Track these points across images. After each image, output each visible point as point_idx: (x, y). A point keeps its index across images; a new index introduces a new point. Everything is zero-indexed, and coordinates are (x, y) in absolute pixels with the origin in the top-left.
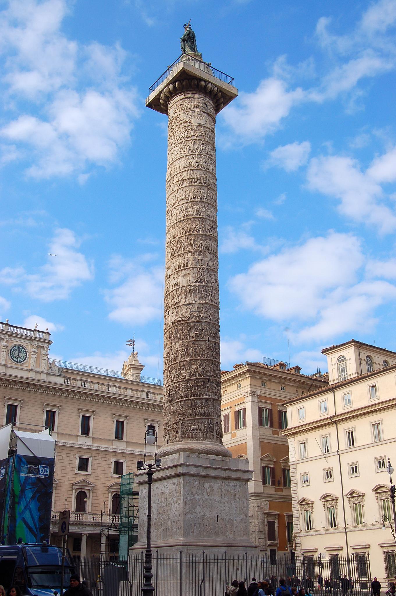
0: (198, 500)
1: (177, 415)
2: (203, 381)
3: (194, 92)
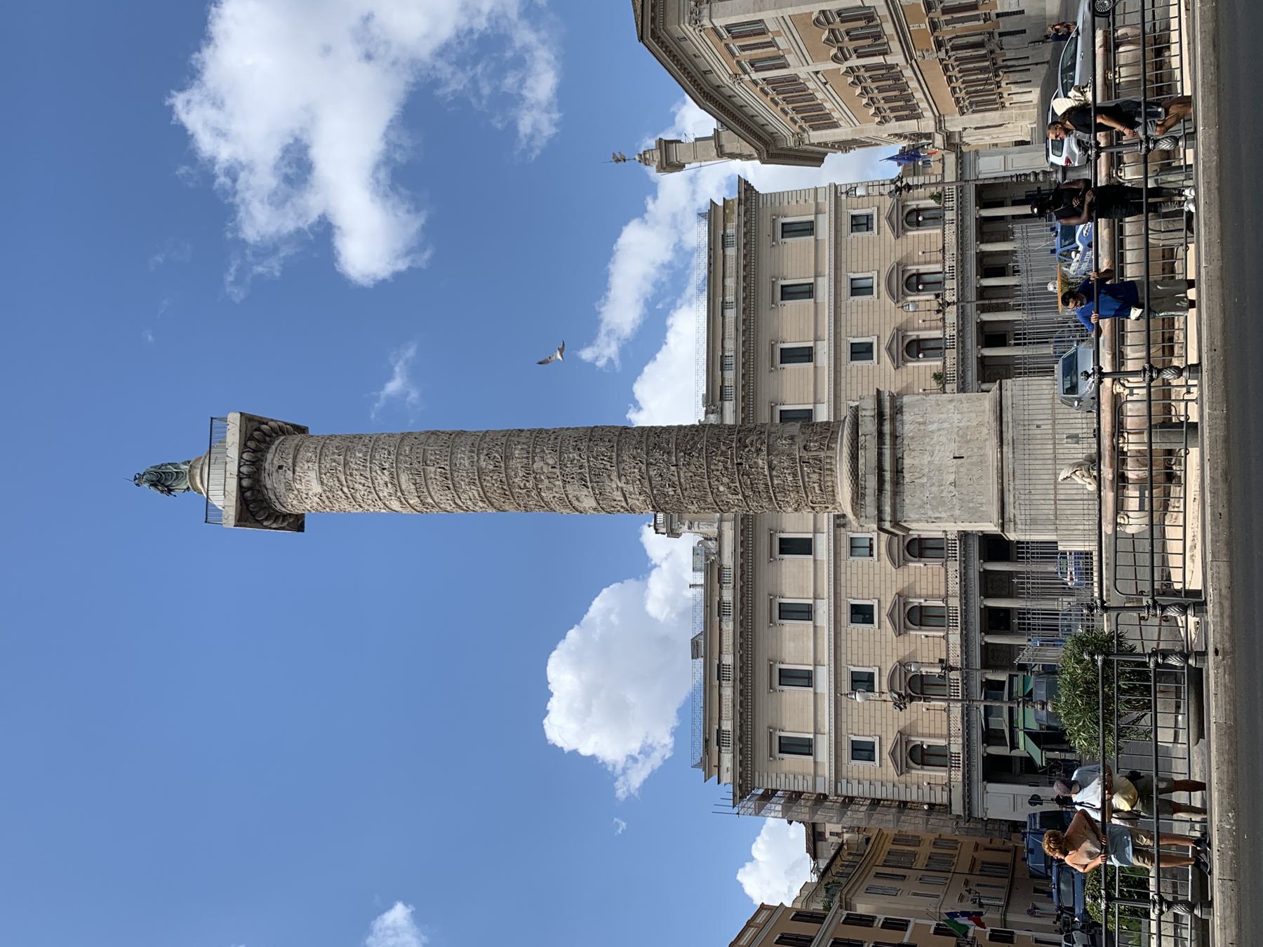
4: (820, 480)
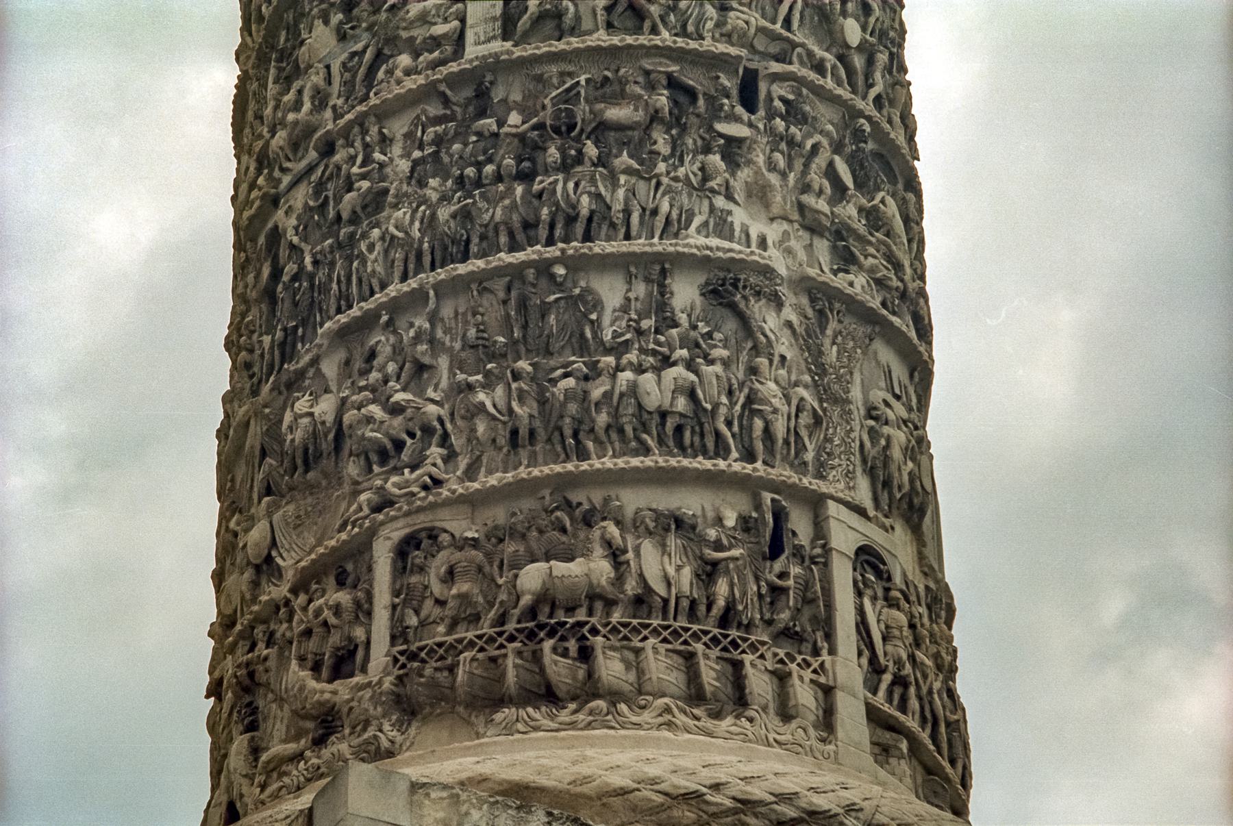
1: (352, 469)
2: (673, 83)
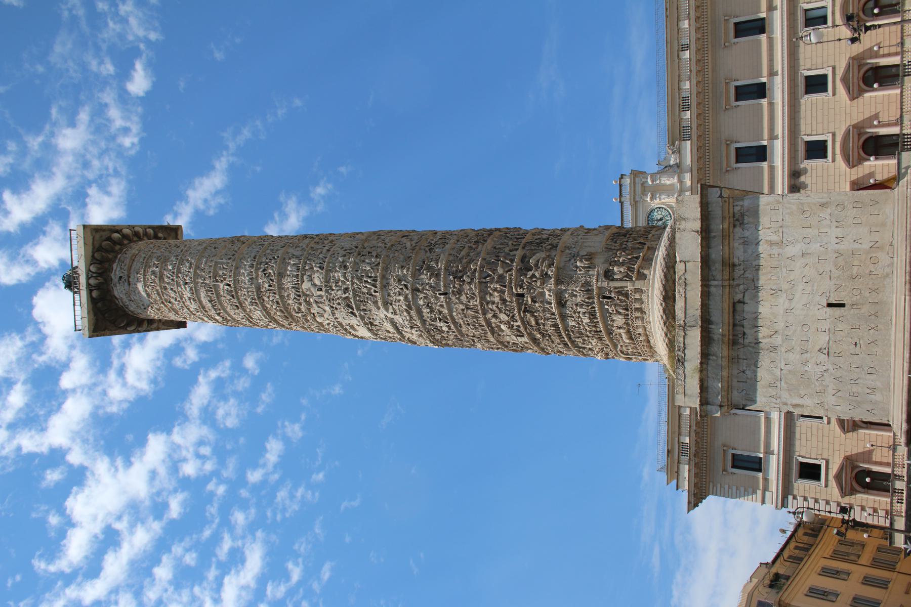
0: (790, 367)
3: (114, 299)
4: (628, 324)
